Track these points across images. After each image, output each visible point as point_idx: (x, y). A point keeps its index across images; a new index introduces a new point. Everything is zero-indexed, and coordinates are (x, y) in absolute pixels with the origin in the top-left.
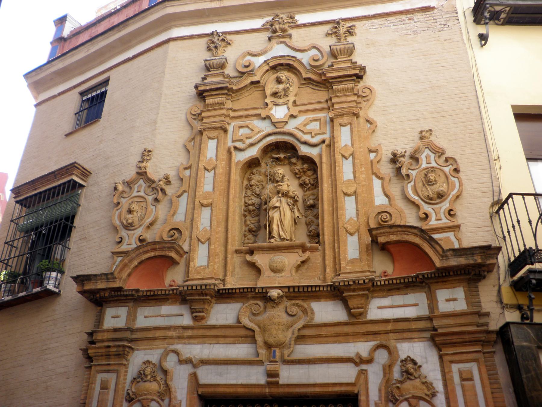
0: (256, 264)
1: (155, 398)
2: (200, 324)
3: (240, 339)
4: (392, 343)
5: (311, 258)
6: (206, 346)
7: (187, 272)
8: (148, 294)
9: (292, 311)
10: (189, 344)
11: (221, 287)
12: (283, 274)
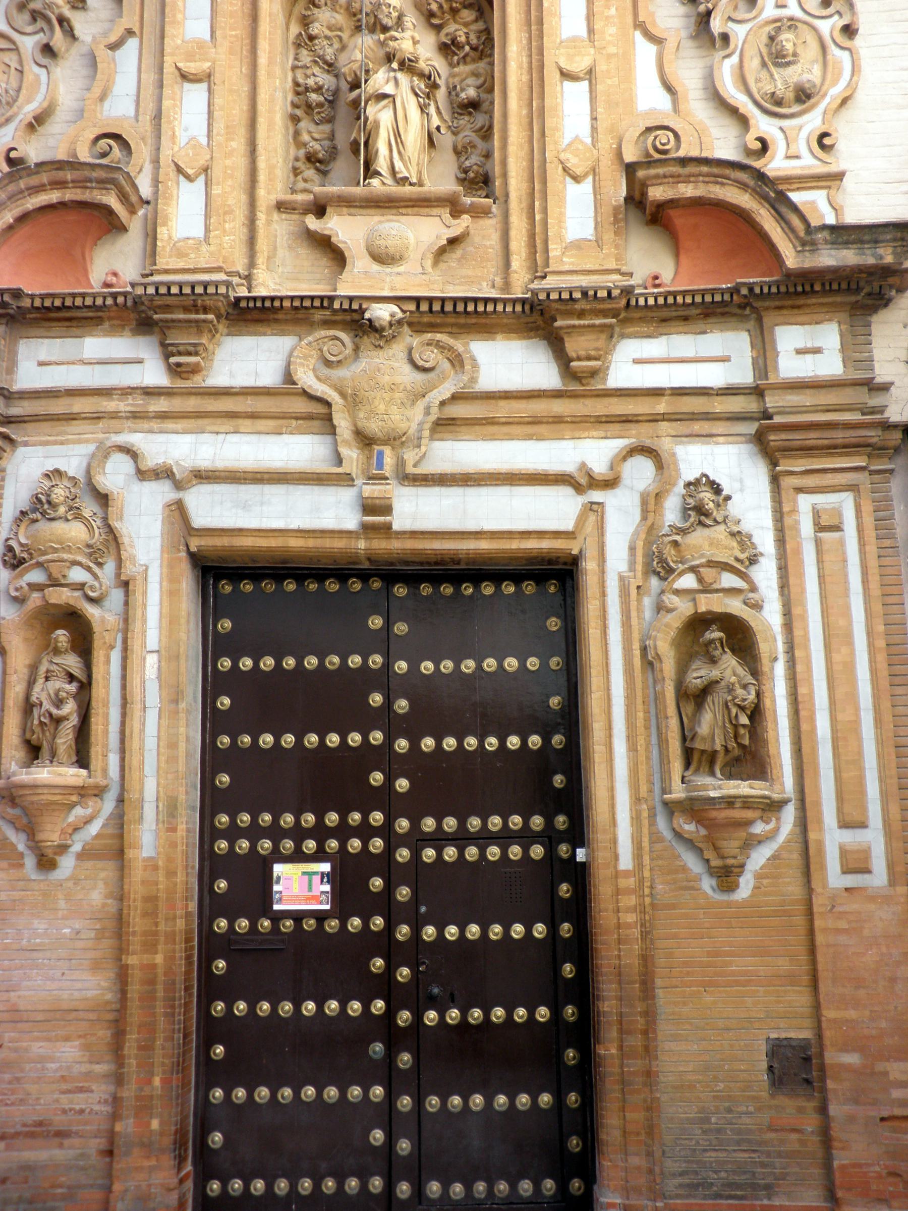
0: (333, 239)
1: (79, 558)
2: (188, 384)
3: (294, 422)
4: (665, 444)
5: (472, 232)
8: (47, 303)
9: (425, 358)
10: (161, 432)
11: (243, 292)
12: (401, 269)
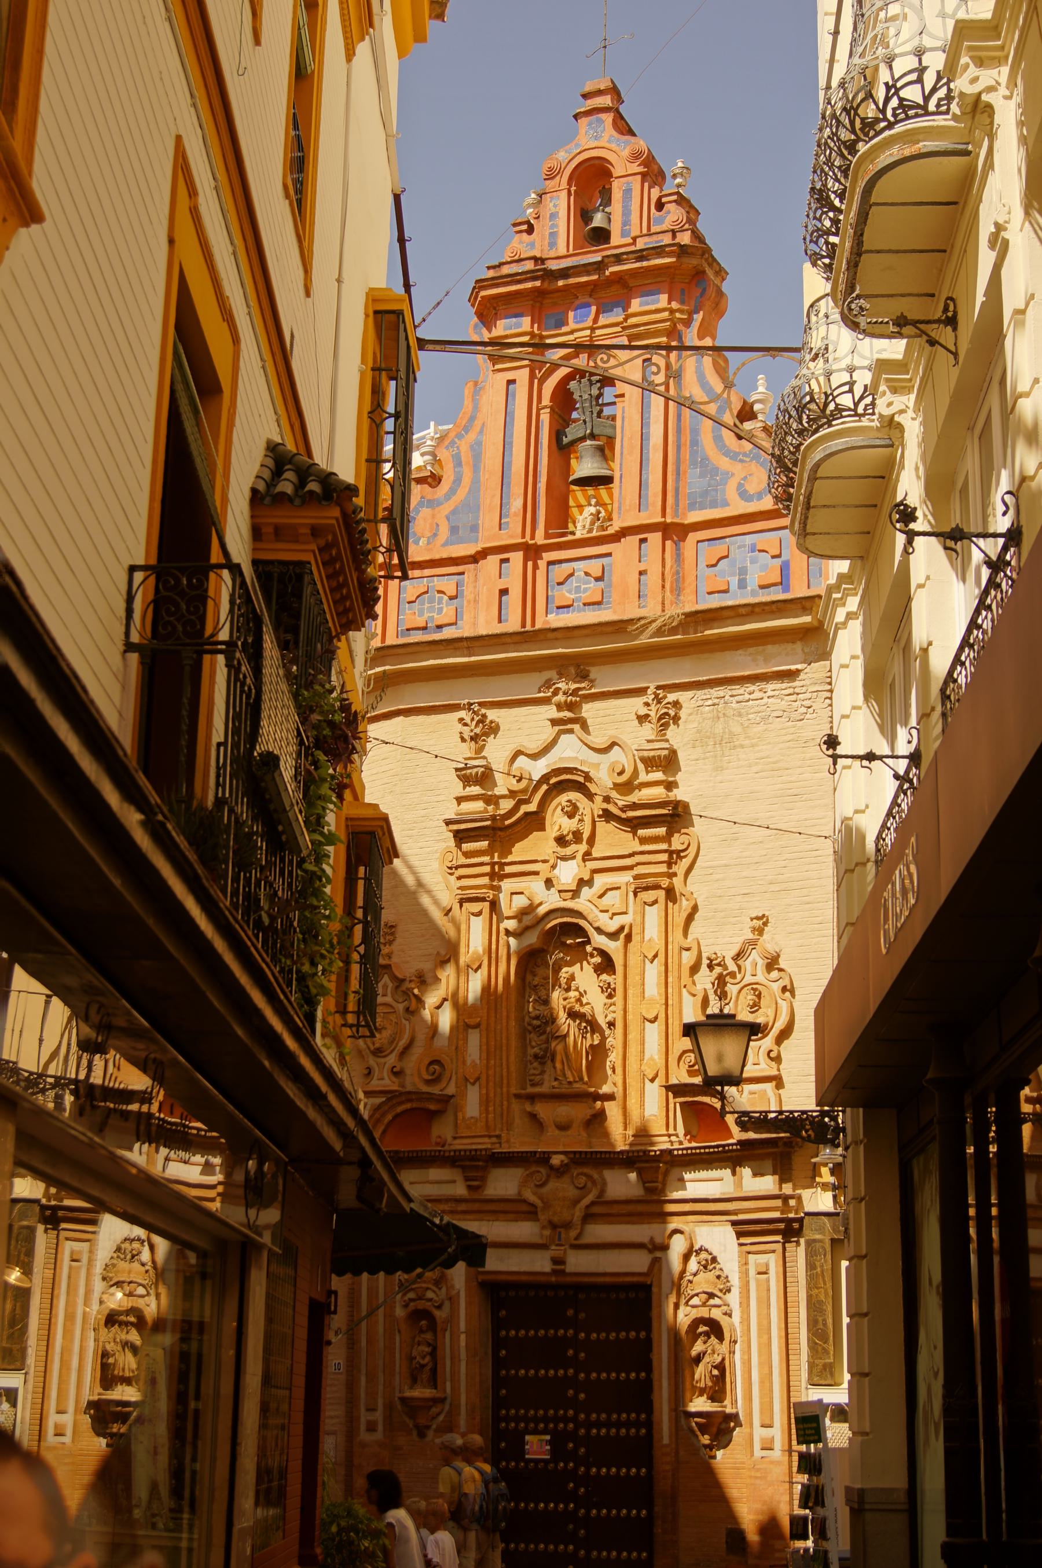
1: (430, 1286)
6: (484, 1223)
7: (456, 1125)
12: (569, 1132)
